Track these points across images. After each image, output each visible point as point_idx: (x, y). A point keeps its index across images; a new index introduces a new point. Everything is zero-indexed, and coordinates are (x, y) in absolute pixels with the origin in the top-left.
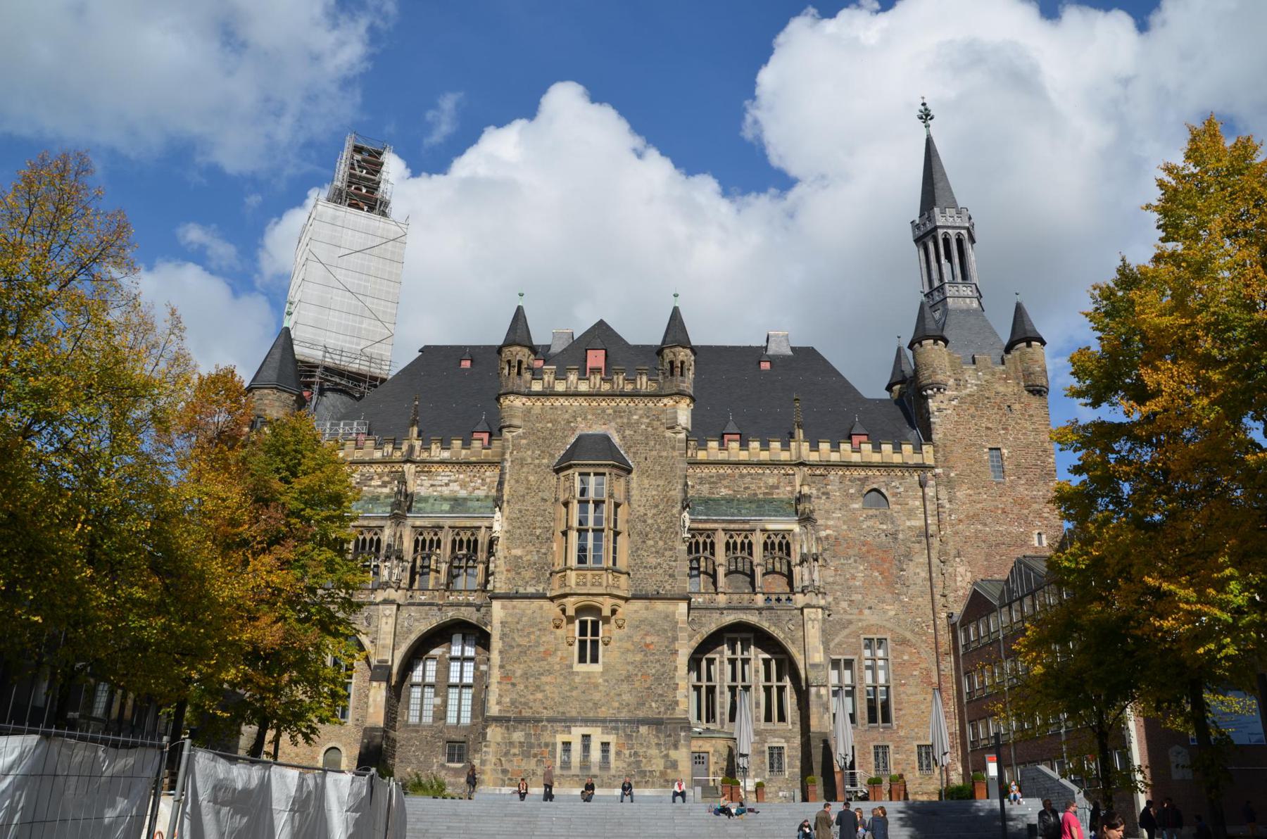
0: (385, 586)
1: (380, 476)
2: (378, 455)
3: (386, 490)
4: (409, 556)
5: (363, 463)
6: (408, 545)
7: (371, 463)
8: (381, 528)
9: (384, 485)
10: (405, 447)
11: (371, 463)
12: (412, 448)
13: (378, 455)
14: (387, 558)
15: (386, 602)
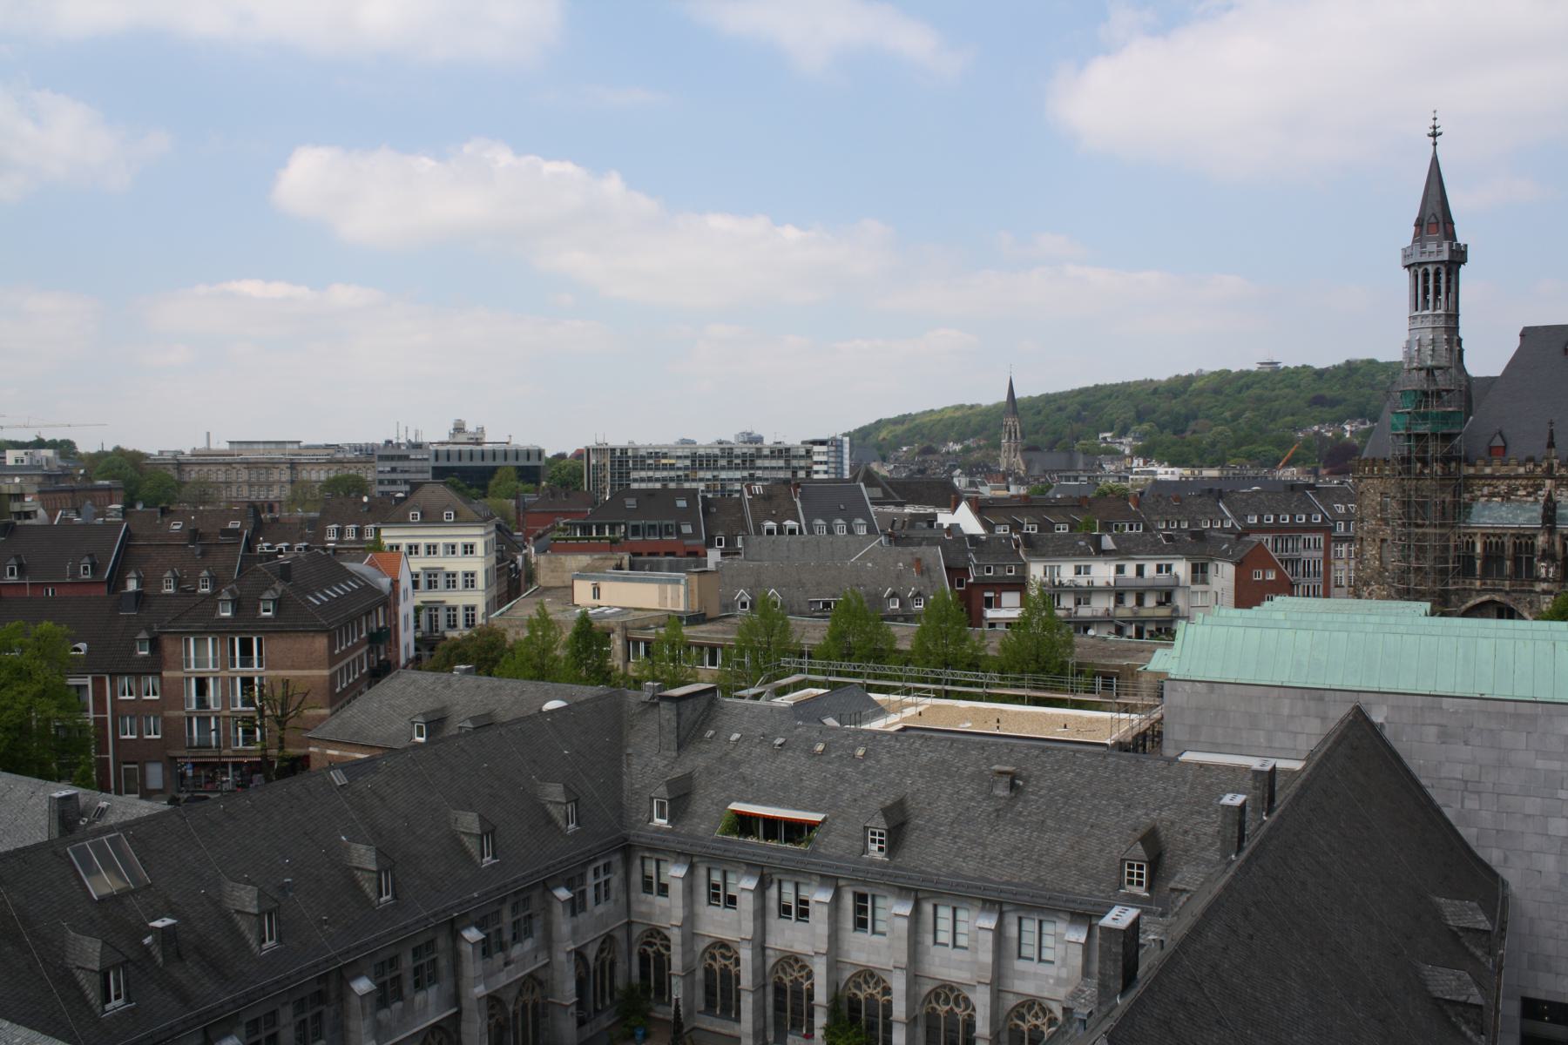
0: (1545, 580)
1: (1525, 488)
2: (1521, 470)
3: (1531, 499)
4: (1560, 556)
5: (1510, 478)
6: (1558, 547)
7: (1517, 477)
8: (1535, 536)
9: (1529, 494)
10: (1545, 465)
11: (1517, 477)
12: (1551, 466)
13: (1521, 470)
14: (1543, 559)
15: (1545, 592)
